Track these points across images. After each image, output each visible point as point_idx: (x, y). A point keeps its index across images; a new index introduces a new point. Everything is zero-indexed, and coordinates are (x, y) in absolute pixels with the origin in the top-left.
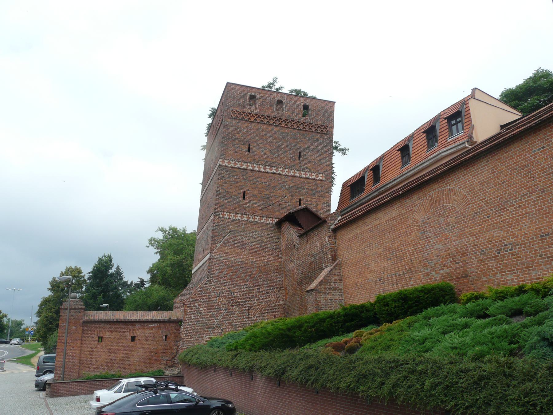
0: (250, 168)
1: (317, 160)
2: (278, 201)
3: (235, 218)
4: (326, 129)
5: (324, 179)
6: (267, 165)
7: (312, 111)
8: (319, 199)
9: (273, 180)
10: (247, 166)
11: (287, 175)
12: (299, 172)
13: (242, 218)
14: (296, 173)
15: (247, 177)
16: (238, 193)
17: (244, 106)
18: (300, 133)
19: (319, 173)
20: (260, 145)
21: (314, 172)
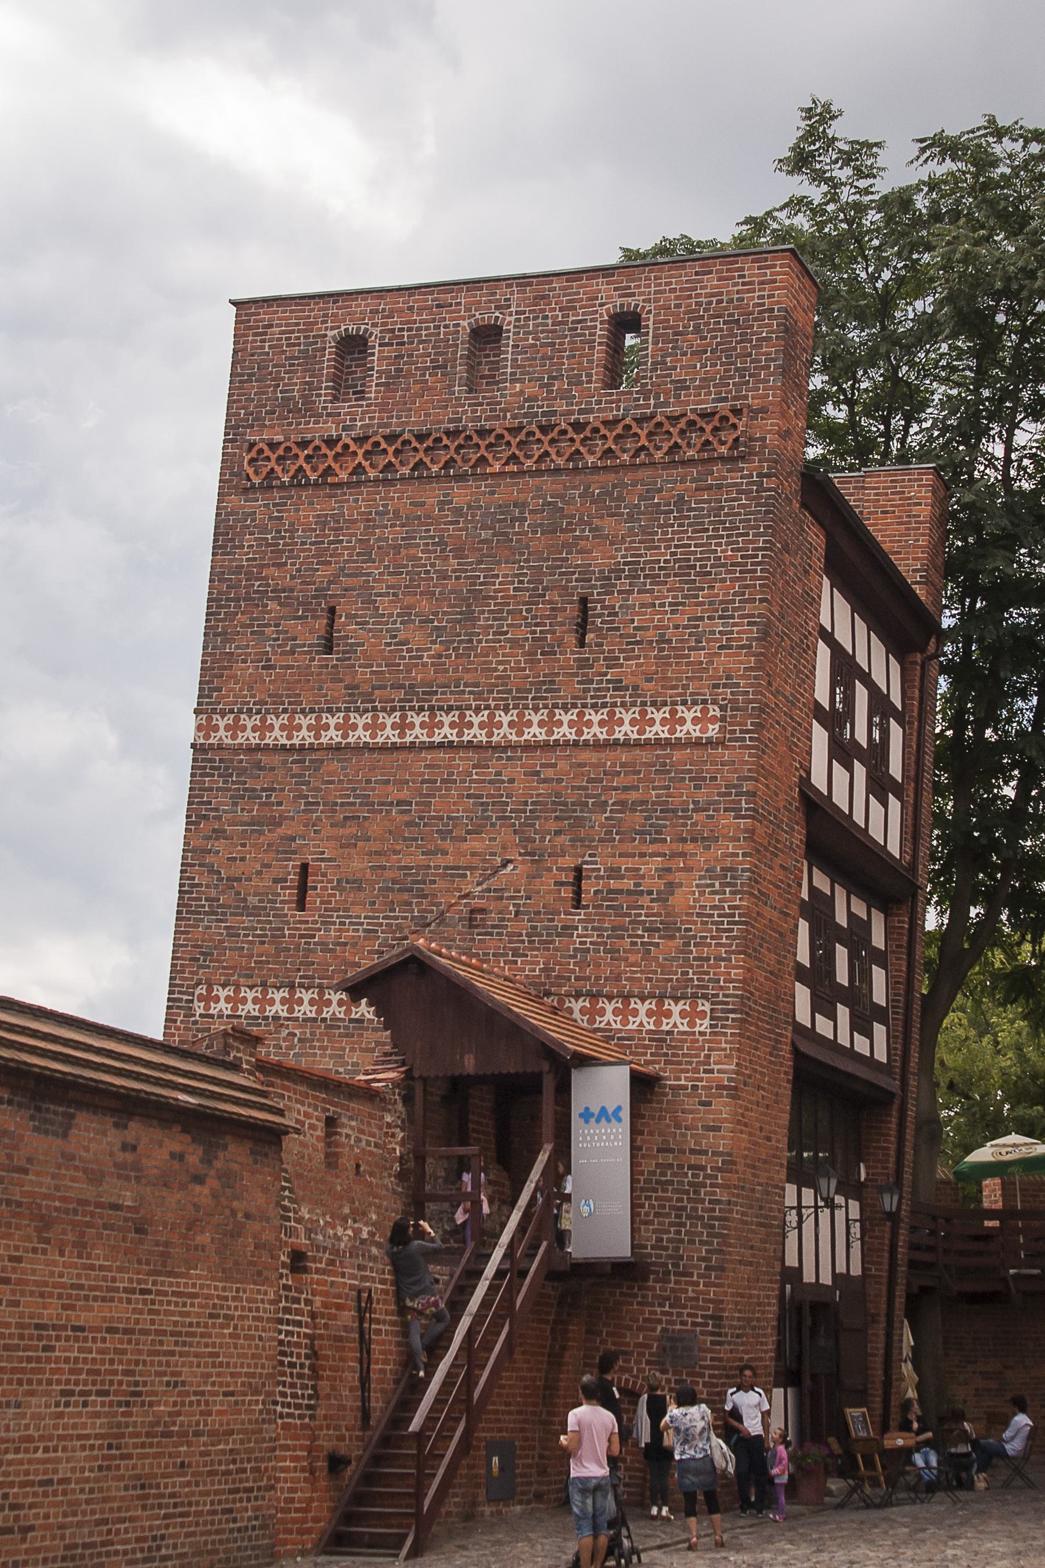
0: (332, 736)
1: (677, 627)
2: (466, 896)
3: (262, 1010)
4: (734, 426)
5: (713, 730)
6: (412, 709)
7: (656, 343)
8: (683, 855)
9: (443, 781)
10: (318, 729)
11: (510, 746)
12: (573, 715)
13: (291, 1010)
14: (560, 723)
15: (317, 789)
16: (276, 881)
17: (309, 409)
18: (587, 488)
19: (684, 703)
20: (384, 604)
21: (654, 704)
